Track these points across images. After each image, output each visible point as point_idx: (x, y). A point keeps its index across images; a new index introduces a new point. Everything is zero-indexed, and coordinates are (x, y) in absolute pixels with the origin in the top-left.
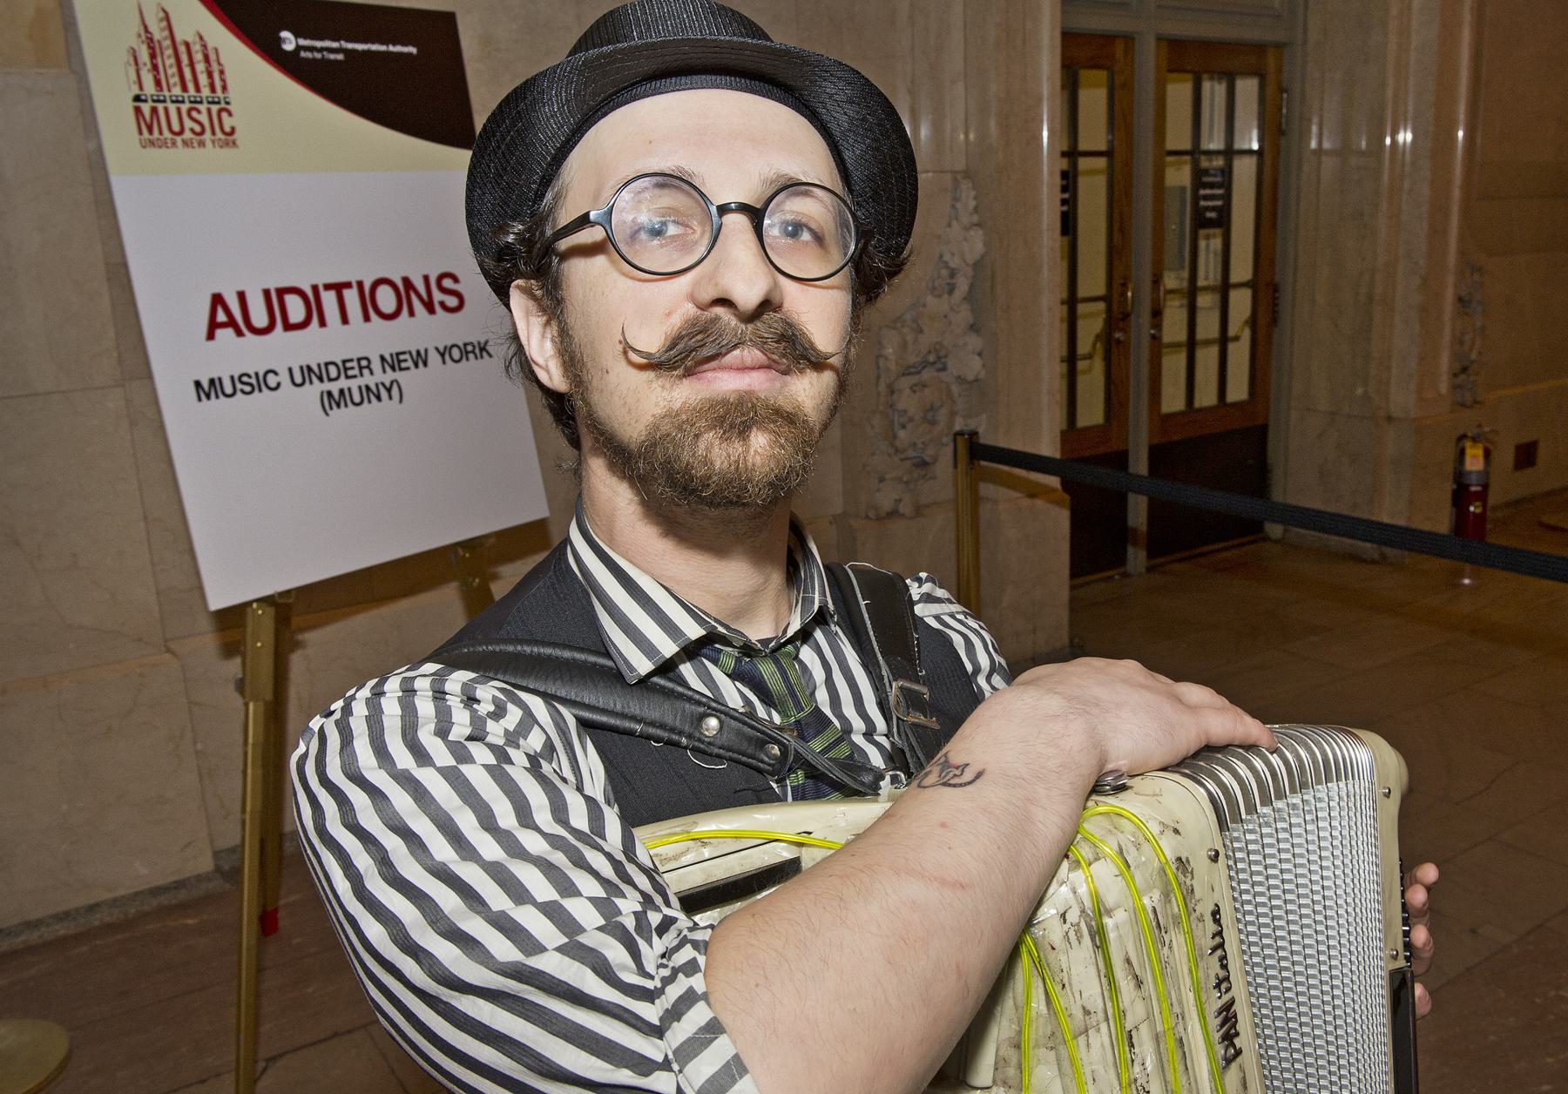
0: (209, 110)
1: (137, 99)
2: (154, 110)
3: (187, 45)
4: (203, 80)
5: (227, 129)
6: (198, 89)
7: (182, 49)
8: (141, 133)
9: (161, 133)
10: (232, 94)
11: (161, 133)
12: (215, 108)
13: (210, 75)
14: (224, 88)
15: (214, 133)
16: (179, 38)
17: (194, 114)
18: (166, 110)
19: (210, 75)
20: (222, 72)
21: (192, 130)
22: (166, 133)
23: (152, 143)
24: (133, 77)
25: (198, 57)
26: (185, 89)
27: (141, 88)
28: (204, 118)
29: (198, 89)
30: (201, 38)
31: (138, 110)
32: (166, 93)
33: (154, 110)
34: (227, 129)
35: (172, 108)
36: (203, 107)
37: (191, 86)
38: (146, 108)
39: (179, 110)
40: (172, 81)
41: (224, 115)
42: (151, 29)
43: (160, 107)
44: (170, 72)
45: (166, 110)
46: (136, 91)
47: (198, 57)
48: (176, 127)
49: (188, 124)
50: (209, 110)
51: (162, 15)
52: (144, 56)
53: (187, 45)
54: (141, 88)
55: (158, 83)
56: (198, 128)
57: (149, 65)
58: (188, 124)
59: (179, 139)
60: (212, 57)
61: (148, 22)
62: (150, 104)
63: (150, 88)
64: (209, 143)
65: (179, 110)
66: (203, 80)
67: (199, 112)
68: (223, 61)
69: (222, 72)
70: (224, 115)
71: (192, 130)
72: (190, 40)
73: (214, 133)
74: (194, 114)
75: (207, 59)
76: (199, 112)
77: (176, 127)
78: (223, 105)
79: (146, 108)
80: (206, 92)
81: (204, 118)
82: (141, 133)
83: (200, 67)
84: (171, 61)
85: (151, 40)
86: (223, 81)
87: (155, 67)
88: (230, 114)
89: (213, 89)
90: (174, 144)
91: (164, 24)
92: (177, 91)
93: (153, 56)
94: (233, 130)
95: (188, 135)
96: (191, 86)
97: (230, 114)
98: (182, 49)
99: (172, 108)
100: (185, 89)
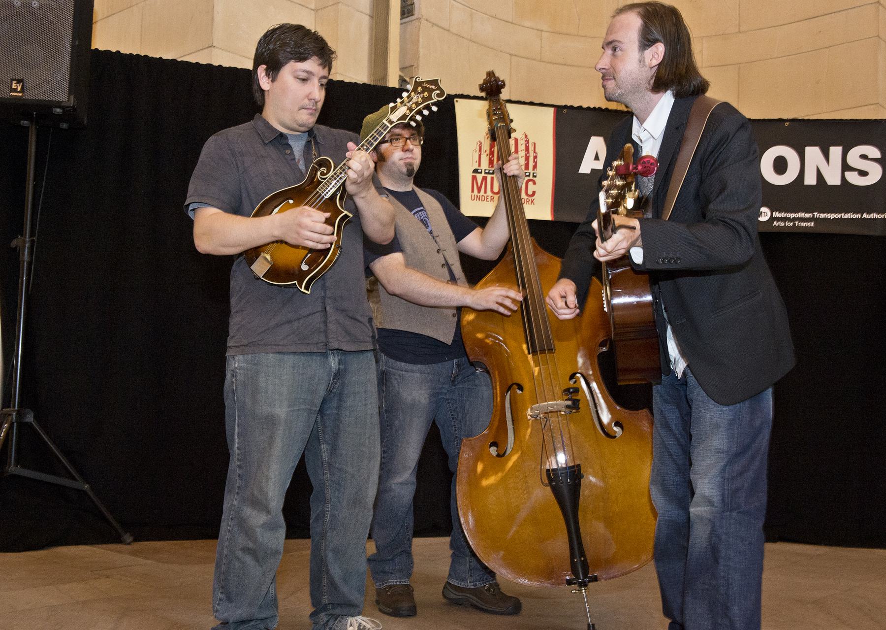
1: (476, 171)
2: (485, 179)
5: (530, 192)
8: (473, 191)
9: (485, 192)
11: (485, 192)
14: (535, 167)
19: (527, 158)
20: (535, 157)
22: (489, 193)
23: (478, 198)
24: (477, 159)
27: (479, 165)
30: (526, 136)
31: (474, 178)
33: (485, 179)
34: (530, 192)
38: (479, 177)
41: (530, 184)
43: (489, 177)
45: (492, 178)
54: (479, 165)
57: (488, 152)
60: (531, 148)
63: (485, 165)
69: (535, 157)
70: (530, 184)
75: (527, 149)
79: (479, 177)
82: (473, 191)
86: (536, 163)
88: (534, 183)
94: (534, 193)
97: (534, 183)
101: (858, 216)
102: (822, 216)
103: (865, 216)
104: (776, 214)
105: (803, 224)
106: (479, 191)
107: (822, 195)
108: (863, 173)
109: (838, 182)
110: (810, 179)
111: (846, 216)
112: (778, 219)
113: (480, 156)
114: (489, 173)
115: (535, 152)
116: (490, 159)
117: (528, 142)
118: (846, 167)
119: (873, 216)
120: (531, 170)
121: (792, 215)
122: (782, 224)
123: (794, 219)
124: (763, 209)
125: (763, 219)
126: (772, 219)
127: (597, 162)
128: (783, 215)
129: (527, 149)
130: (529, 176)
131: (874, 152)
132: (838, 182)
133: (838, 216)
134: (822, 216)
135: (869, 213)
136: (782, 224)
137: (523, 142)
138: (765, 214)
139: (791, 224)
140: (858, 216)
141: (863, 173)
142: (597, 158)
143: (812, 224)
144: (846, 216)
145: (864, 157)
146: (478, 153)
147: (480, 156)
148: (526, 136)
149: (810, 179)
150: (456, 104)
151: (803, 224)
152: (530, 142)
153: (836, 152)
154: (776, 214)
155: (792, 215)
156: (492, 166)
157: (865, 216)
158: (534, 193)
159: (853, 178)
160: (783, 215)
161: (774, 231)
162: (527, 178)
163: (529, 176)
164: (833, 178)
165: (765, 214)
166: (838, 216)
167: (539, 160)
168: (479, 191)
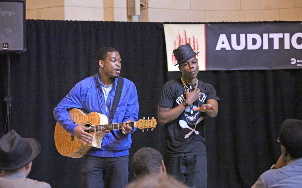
3: (189, 39)
8: (173, 61)
16: (188, 38)
20: (198, 45)
30: (193, 37)
42: (180, 36)
51: (184, 32)
53: (189, 39)
68: (198, 42)
69: (198, 45)
72: (190, 38)
75: (194, 42)
82: (173, 61)
85: (180, 38)
86: (198, 47)
91: (184, 34)
104: (298, 61)
113: (175, 46)
115: (197, 43)
117: (194, 39)
124: (292, 59)
125: (293, 63)
126: (297, 63)
127: (223, 44)
129: (194, 42)
138: (294, 61)
142: (223, 43)
146: (174, 45)
147: (175, 46)
148: (193, 37)
154: (298, 61)
161: (298, 68)
165: (294, 61)
167: (199, 46)
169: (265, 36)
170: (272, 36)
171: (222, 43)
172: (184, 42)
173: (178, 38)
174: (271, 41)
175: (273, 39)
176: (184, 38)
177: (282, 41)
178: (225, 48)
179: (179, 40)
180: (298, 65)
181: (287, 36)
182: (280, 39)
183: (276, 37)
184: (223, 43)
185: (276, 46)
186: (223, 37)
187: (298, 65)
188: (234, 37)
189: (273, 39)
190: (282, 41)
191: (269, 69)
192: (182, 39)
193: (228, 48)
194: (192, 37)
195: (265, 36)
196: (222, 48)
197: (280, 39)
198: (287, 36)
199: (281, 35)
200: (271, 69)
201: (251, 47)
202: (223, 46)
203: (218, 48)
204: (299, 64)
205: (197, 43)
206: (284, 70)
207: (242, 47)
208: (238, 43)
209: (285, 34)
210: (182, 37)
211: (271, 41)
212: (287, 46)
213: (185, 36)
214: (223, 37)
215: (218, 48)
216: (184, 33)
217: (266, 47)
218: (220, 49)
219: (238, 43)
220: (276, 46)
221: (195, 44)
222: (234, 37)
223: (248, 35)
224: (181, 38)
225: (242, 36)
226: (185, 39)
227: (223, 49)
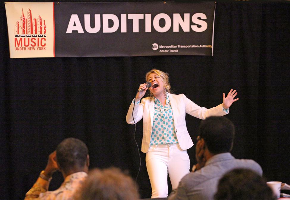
0: (38, 39)
1: (16, 36)
2: (21, 39)
3: (35, 20)
4: (39, 30)
5: (43, 44)
6: (36, 33)
7: (34, 21)
8: (15, 46)
9: (22, 46)
10: (47, 34)
11: (22, 46)
12: (40, 38)
13: (41, 28)
14: (45, 32)
15: (38, 46)
16: (33, 18)
17: (33, 40)
18: (25, 39)
19: (41, 28)
20: (45, 27)
21: (32, 45)
23: (18, 49)
24: (17, 30)
25: (38, 23)
26: (32, 33)
27: (18, 33)
28: (36, 41)
29: (36, 33)
30: (40, 17)
31: (16, 39)
32: (26, 34)
33: (21, 39)
34: (43, 44)
35: (27, 38)
36: (36, 38)
37: (34, 32)
38: (18, 39)
39: (29, 39)
40: (28, 31)
41: (43, 40)
42: (25, 16)
43: (23, 38)
44: (28, 28)
45: (25, 39)
46: (16, 34)
47: (38, 23)
48: (27, 44)
49: (31, 43)
50: (38, 39)
51: (29, 11)
52: (21, 24)
53: (35, 20)
54: (18, 33)
55: (24, 31)
56: (33, 44)
57: (22, 26)
58: (31, 43)
59: (27, 48)
60: (43, 23)
61: (24, 14)
62: (20, 37)
63: (21, 33)
64: (36, 49)
65: (29, 39)
66: (39, 30)
67: (35, 39)
68: (45, 24)
69: (45, 27)
70: (43, 40)
71: (32, 45)
72: (36, 18)
73: (38, 46)
74: (33, 40)
76: (35, 39)
77: (27, 44)
78: (43, 37)
80: (39, 33)
81: (36, 41)
82: (15, 46)
83: (38, 26)
84: (29, 25)
85: (25, 19)
86: (45, 30)
87: (24, 27)
88: (45, 40)
89: (41, 32)
90: (25, 49)
91: (30, 14)
92: (29, 33)
93: (24, 24)
94: (45, 44)
95: (30, 46)
96: (34, 32)
97: (45, 40)
98: (34, 21)
99: (27, 38)
100: (32, 33)
101: (197, 46)
102: (182, 47)
103: (200, 46)
104: (161, 47)
105: (173, 51)
106: (19, 46)
107: (182, 37)
108: (199, 26)
109: (188, 30)
110: (176, 29)
111: (192, 47)
112: (162, 49)
113: (18, 28)
114: (23, 37)
115: (45, 25)
116: (23, 30)
117: (41, 20)
118: (192, 23)
119: (204, 46)
120: (43, 34)
121: (168, 47)
122: (163, 51)
123: (169, 49)
124: (154, 45)
126: (159, 49)
128: (164, 47)
130: (42, 37)
131: (204, 16)
132: (188, 30)
133: (189, 47)
134: (182, 47)
135: (202, 45)
136: (163, 51)
137: (39, 20)
138: (156, 46)
139: (168, 51)
140: (197, 46)
141: (199, 26)
142: (75, 25)
143: (177, 51)
144: (192, 47)
145: (199, 18)
146: (17, 28)
147: (18, 28)
148: (40, 17)
149: (176, 29)
150: (5, 4)
151: (173, 51)
152: (42, 20)
153: (187, 16)
154: (161, 47)
155: (168, 47)
156: (24, 33)
157: (200, 46)
158: (45, 44)
159: (195, 28)
160: (164, 47)
161: (161, 55)
162: (42, 38)
163: (42, 37)
164: (186, 29)
165: (156, 46)
166: (189, 47)
167: (47, 29)
168: (19, 46)
169: (123, 17)
170: (131, 16)
171: (74, 25)
172: (29, 24)
173: (22, 18)
174: (130, 23)
175: (132, 20)
176: (29, 18)
177: (142, 23)
178: (77, 31)
179: (23, 21)
180: (160, 51)
181: (148, 16)
182: (139, 20)
183: (136, 18)
184: (75, 25)
185: (136, 29)
186: (75, 18)
187: (160, 51)
188: (87, 17)
189: (132, 20)
190: (142, 23)
191: (128, 56)
192: (27, 19)
193: (81, 31)
194: (39, 17)
195: (123, 17)
196: (73, 31)
197: (139, 20)
198: (148, 16)
199: (141, 16)
200: (130, 56)
201: (107, 30)
202: (75, 29)
203: (69, 30)
204: (161, 50)
205: (45, 25)
206: (146, 57)
207: (96, 30)
208: (93, 25)
209: (146, 15)
210: (27, 17)
211: (130, 23)
212: (148, 29)
213: (30, 17)
214: (75, 18)
215: (69, 30)
216: (29, 13)
217: (124, 30)
218: (71, 32)
219: (93, 25)
220: (136, 29)
221: (40, 26)
222: (87, 17)
223: (103, 15)
224: (26, 19)
225: (97, 17)
226: (30, 19)
227: (75, 32)
